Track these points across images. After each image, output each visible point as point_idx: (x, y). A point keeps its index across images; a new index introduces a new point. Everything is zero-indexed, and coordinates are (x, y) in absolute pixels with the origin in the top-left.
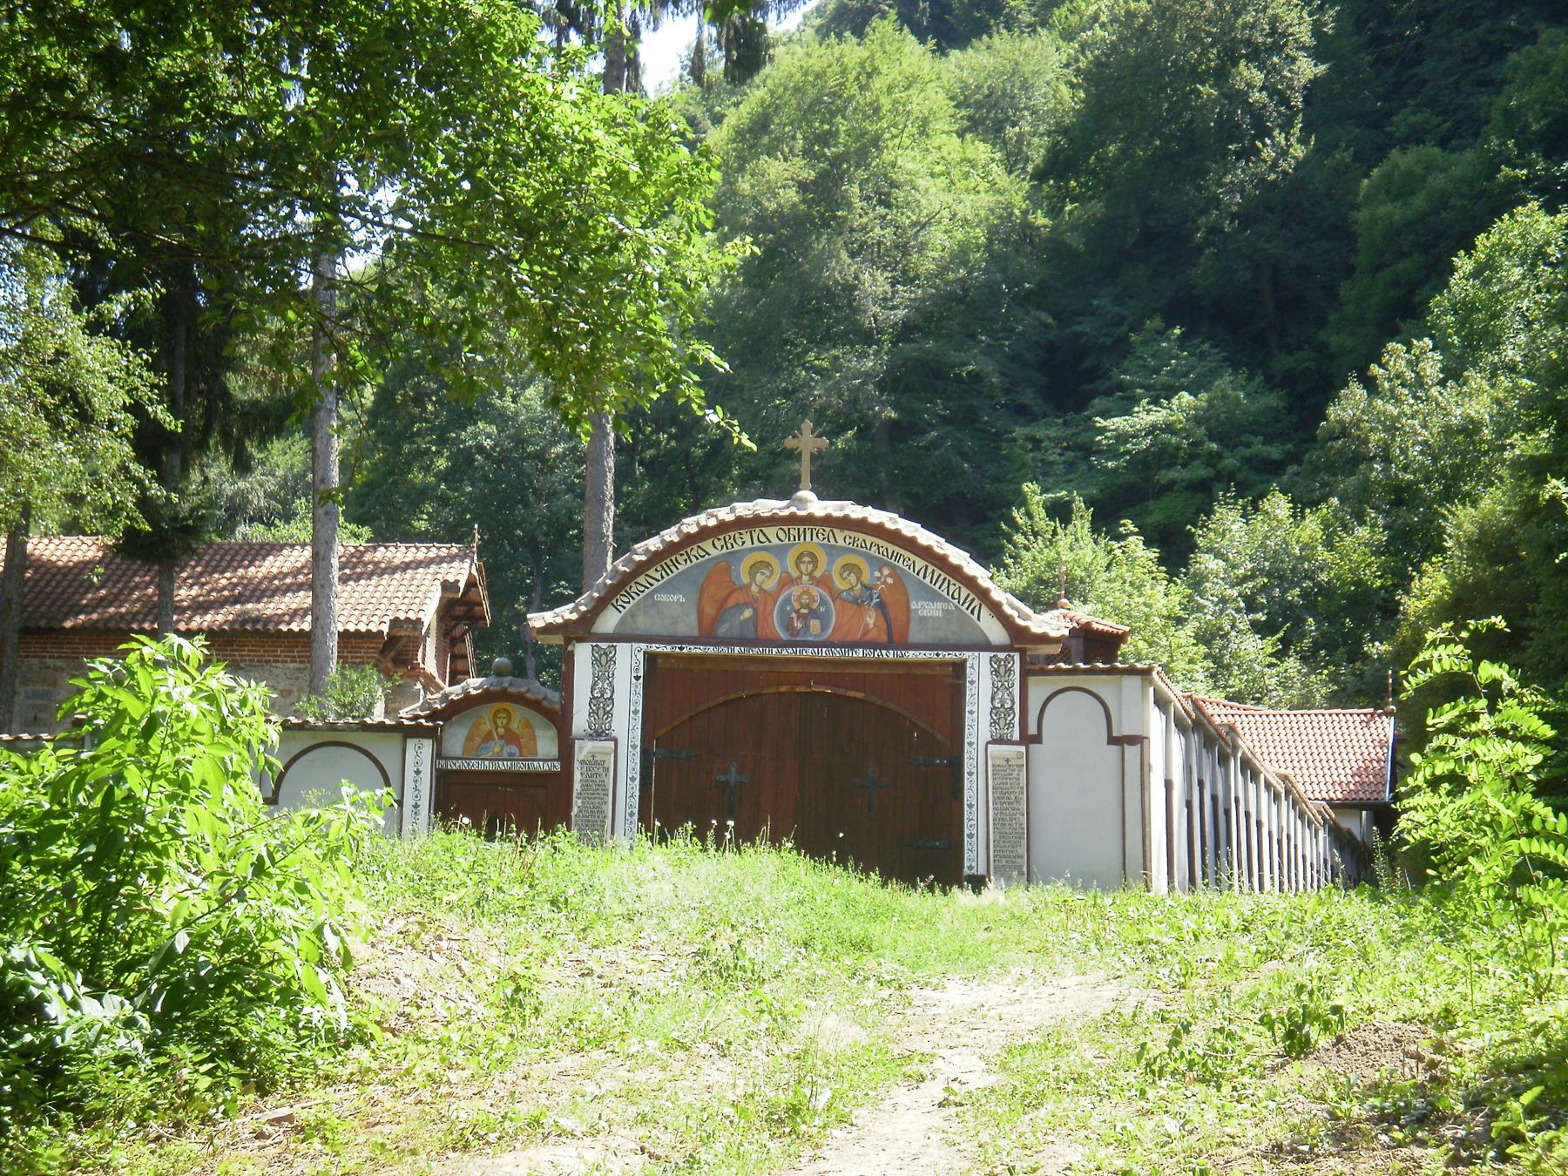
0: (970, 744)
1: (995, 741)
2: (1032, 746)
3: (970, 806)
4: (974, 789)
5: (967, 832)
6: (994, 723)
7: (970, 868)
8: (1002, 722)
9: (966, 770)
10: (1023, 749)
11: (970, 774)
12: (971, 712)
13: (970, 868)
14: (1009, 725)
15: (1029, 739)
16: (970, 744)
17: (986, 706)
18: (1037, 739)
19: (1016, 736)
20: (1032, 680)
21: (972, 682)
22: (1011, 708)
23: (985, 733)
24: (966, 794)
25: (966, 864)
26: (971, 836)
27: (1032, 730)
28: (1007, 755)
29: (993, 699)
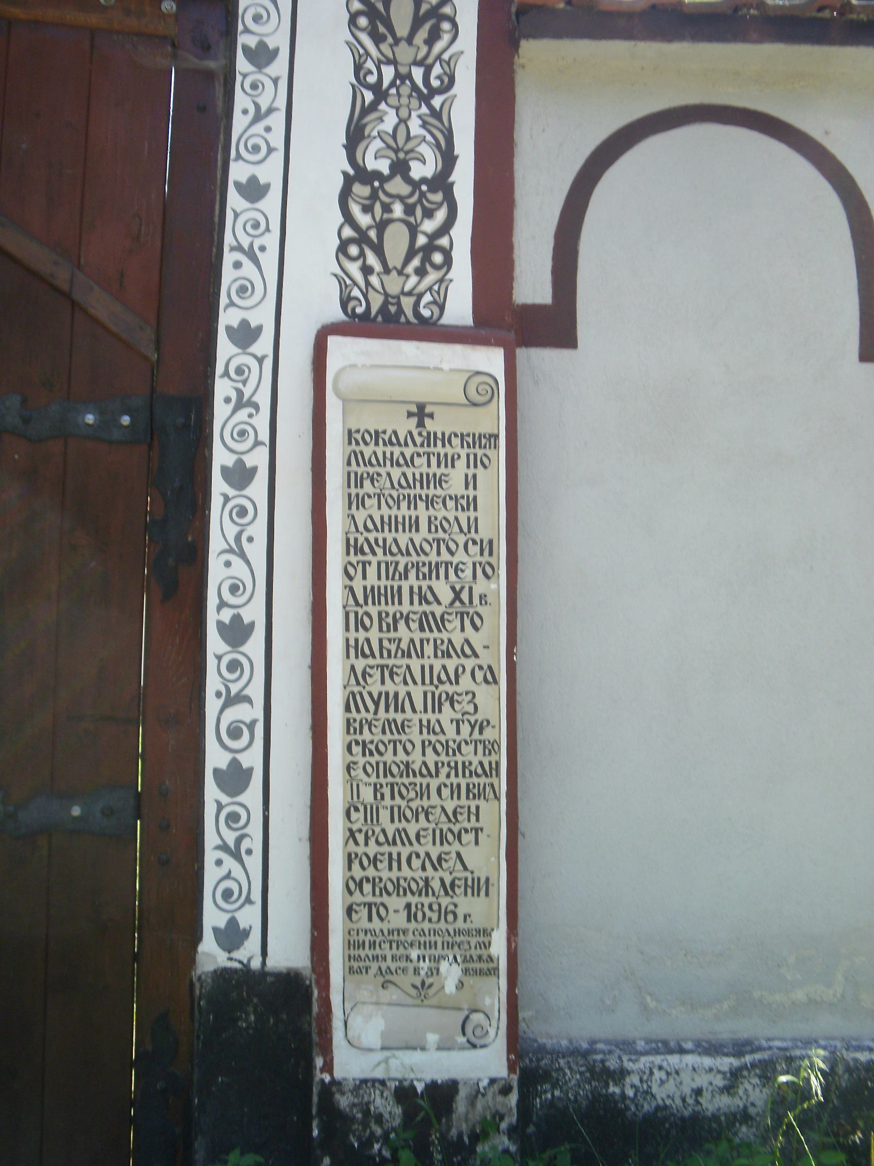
0: (245, 335)
1: (359, 324)
2: (538, 359)
3: (236, 632)
4: (254, 553)
5: (215, 757)
6: (357, 242)
7: (231, 936)
8: (396, 241)
9: (221, 457)
10: (490, 360)
11: (240, 476)
12: (254, 190)
13: (231, 936)
14: (430, 254)
15: (503, 320)
16: (245, 335)
17: (321, 165)
18: (553, 325)
19: (460, 307)
20: (536, 54)
21: (262, 56)
22: (441, 182)
23: (315, 288)
24: (217, 572)
25: (213, 917)
26: (234, 779)
27: (533, 285)
28: (420, 388)
29: (355, 137)
